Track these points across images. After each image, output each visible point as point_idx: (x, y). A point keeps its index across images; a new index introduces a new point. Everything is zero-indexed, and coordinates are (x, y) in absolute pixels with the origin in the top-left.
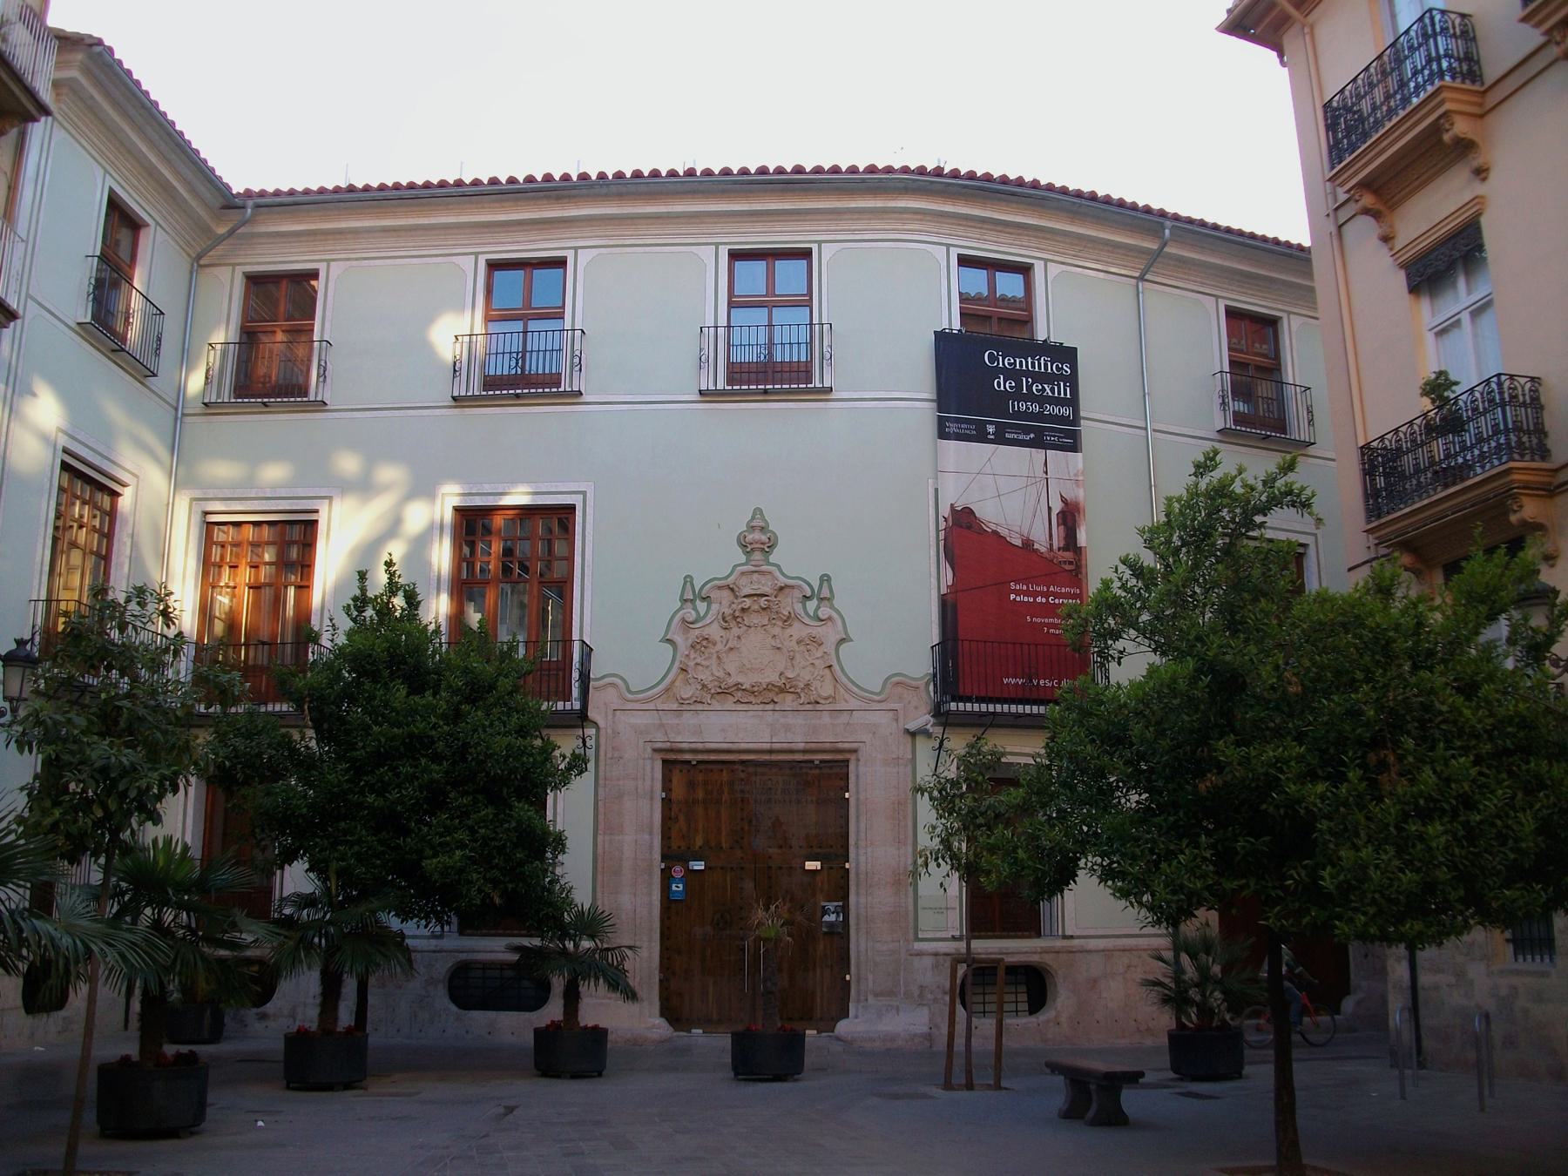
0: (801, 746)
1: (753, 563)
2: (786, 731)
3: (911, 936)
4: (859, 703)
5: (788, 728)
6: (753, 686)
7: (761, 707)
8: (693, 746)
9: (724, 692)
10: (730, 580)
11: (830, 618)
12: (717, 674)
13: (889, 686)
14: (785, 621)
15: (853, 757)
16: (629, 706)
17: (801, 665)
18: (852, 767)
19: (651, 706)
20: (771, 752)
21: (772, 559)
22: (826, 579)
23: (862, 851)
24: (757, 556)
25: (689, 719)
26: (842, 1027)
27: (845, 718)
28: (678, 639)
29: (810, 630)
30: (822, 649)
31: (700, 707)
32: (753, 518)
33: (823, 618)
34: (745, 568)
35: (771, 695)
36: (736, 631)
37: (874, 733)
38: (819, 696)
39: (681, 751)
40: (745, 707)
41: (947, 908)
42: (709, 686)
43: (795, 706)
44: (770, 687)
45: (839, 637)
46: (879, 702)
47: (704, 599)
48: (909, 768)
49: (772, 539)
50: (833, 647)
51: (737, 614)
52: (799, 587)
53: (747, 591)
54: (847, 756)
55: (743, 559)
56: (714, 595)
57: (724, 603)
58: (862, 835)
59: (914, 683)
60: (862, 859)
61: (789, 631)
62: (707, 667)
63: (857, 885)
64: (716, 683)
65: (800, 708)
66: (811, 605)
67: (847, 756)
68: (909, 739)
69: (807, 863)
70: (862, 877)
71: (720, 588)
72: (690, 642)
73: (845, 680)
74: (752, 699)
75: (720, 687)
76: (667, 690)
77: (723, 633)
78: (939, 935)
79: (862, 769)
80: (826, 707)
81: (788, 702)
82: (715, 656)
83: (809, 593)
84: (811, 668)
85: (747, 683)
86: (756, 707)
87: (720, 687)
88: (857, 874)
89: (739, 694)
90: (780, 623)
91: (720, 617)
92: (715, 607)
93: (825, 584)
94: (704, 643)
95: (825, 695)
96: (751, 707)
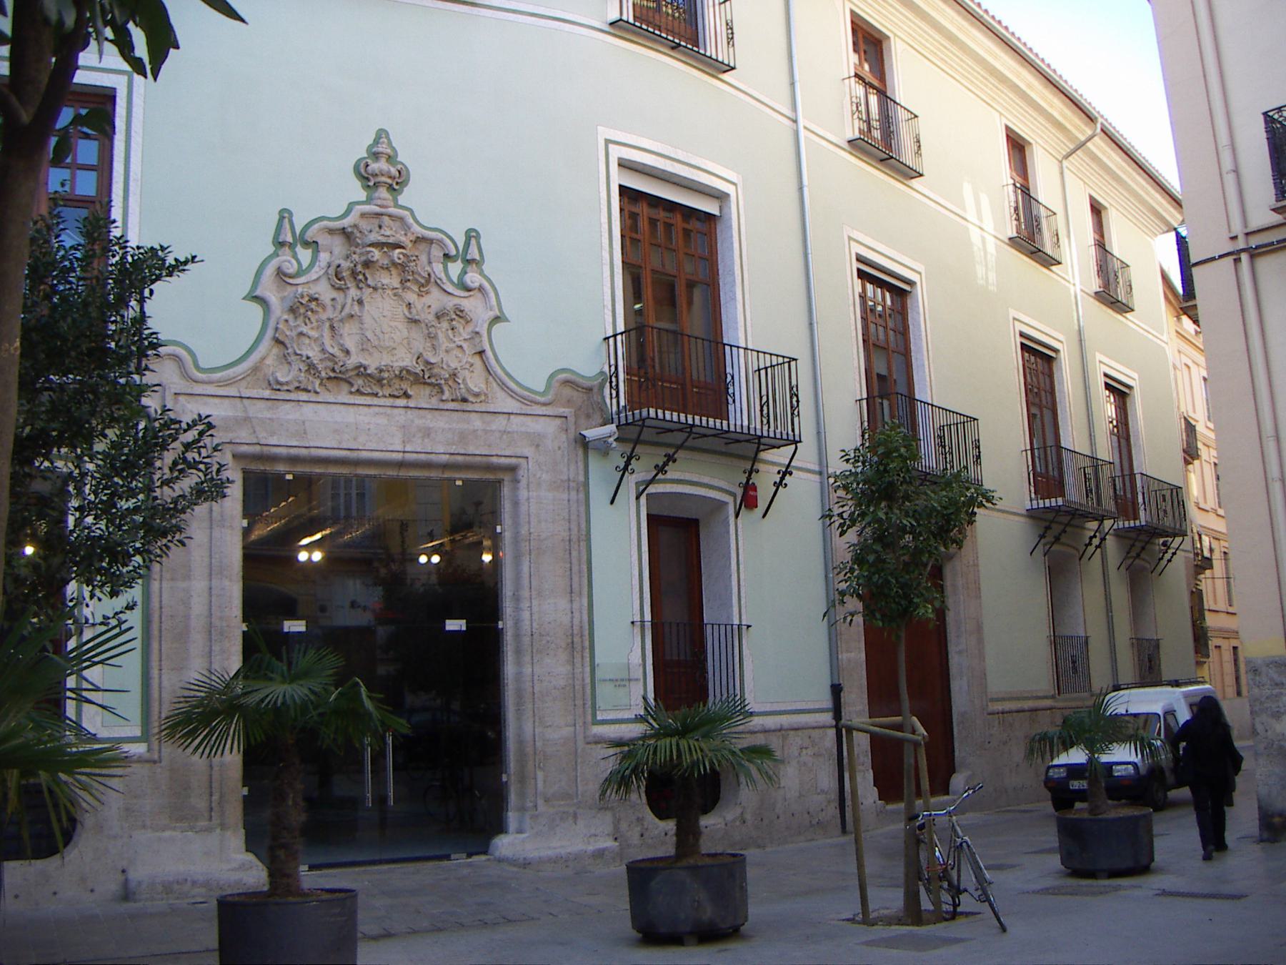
0: (445, 458)
1: (379, 202)
2: (423, 437)
3: (589, 718)
4: (518, 404)
5: (427, 433)
6: (381, 371)
7: (389, 401)
8: (293, 451)
9: (338, 377)
10: (346, 222)
11: (481, 289)
12: (331, 350)
13: (555, 384)
14: (423, 286)
15: (507, 478)
16: (198, 389)
17: (444, 348)
18: (506, 491)
19: (232, 391)
20: (401, 464)
21: (402, 200)
22: (472, 235)
23: (525, 604)
24: (383, 193)
25: (288, 413)
26: (504, 844)
27: (500, 423)
28: (274, 299)
29: (457, 301)
30: (470, 328)
31: (304, 396)
32: (377, 141)
33: (472, 285)
34: (367, 208)
35: (405, 386)
36: (353, 292)
37: (538, 446)
38: (469, 390)
39: (274, 459)
40: (368, 400)
41: (630, 680)
42: (320, 367)
43: (434, 402)
44: (404, 374)
45: (491, 314)
46: (545, 404)
47: (306, 244)
48: (582, 496)
49: (404, 173)
50: (486, 326)
51: (359, 268)
52: (440, 242)
53: (374, 237)
54: (500, 476)
55: (362, 195)
56: (323, 240)
57: (334, 251)
58: (526, 582)
59: (588, 384)
60: (526, 615)
61: (427, 300)
62: (316, 340)
63: (518, 652)
64: (330, 364)
65: (442, 406)
66: (455, 268)
67: (500, 476)
68: (580, 452)
69: (448, 622)
70: (526, 640)
71: (331, 231)
72: (288, 304)
73: (499, 371)
74: (376, 389)
75: (333, 370)
76: (255, 369)
77: (334, 294)
78: (620, 715)
79: (523, 494)
80: (477, 407)
81: (422, 396)
82: (327, 324)
83: (453, 252)
84: (457, 352)
85: (372, 364)
86: (382, 401)
87: (333, 370)
88: (517, 636)
89: (359, 382)
90: (415, 288)
91: (332, 271)
92: (324, 257)
93: (473, 241)
94: (313, 305)
95: (476, 390)
96: (375, 401)
